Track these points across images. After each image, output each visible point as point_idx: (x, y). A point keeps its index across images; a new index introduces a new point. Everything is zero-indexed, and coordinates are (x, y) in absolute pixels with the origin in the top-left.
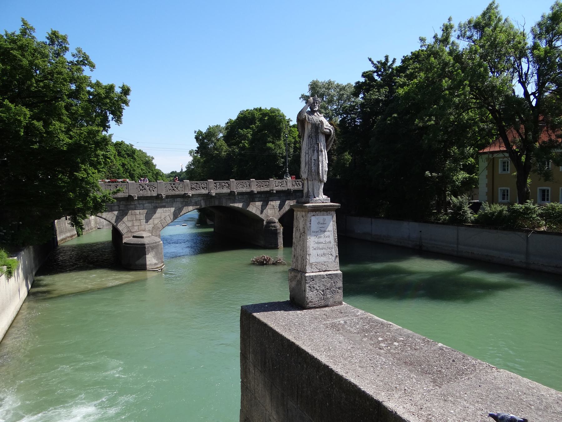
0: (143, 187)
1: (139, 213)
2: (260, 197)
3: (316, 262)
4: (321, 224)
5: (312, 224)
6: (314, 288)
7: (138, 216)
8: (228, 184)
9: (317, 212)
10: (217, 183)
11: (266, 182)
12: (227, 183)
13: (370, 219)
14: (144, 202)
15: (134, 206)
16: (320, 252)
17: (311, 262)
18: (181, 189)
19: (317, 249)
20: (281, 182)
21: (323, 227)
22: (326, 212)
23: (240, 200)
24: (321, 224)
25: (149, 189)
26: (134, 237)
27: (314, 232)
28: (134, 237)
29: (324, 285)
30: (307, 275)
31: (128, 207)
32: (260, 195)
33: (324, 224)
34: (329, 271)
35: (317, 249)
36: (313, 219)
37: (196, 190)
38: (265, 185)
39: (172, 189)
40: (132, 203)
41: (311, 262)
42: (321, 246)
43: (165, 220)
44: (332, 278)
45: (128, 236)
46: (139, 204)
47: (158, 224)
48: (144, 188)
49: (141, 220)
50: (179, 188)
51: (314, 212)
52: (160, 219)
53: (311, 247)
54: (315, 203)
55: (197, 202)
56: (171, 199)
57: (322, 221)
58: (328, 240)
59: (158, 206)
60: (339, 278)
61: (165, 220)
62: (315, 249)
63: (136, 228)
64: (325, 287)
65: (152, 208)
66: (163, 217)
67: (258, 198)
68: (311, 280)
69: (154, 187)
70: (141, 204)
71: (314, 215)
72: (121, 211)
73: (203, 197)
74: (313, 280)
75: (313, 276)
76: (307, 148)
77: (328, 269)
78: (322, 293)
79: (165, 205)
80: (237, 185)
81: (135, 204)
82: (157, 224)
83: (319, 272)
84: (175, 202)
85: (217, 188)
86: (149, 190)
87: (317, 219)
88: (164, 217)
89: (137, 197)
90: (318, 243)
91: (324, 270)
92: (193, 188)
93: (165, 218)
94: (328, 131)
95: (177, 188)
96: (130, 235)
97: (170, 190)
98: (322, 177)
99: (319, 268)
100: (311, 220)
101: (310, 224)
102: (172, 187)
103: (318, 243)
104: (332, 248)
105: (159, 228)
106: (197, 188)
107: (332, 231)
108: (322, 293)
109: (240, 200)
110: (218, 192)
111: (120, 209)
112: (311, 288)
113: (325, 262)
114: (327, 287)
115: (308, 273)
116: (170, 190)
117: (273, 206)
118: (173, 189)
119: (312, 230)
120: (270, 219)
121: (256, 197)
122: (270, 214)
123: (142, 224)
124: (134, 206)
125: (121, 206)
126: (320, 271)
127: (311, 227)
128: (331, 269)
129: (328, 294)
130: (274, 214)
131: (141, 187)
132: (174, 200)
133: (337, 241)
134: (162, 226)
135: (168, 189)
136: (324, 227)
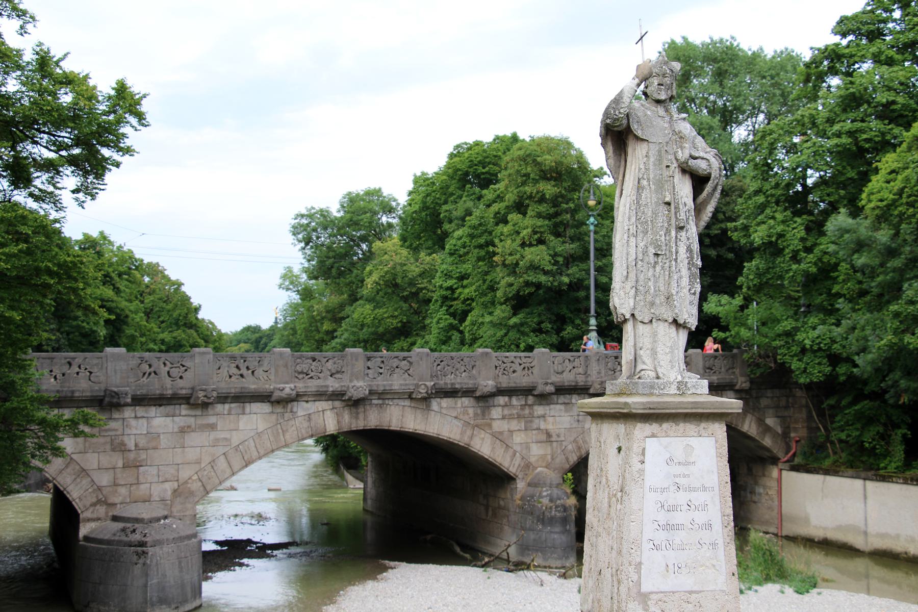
0: (150, 366)
1: (136, 445)
2: (506, 405)
3: (662, 592)
5: (647, 465)
7: (132, 456)
8: (408, 361)
10: (375, 357)
11: (525, 357)
12: (404, 359)
13: (859, 483)
14: (153, 411)
15: (120, 422)
17: (645, 588)
18: (265, 375)
19: (664, 548)
20: (572, 359)
21: (684, 476)
23: (444, 411)
25: (168, 372)
26: (115, 519)
28: (115, 519)
32: (507, 398)
33: (687, 464)
35: (664, 548)
36: (652, 445)
37: (311, 378)
38: (522, 366)
39: (239, 373)
40: (116, 415)
42: (679, 537)
43: (212, 467)
45: (95, 516)
46: (136, 417)
47: (190, 481)
48: (152, 369)
49: (141, 468)
50: (259, 372)
52: (197, 467)
53: (645, 539)
55: (312, 416)
56: (233, 405)
57: (679, 455)
58: (700, 517)
59: (193, 426)
61: (212, 467)
62: (657, 547)
63: (123, 491)
65: (176, 430)
66: (206, 460)
67: (500, 409)
69: (183, 366)
71: (653, 436)
73: (330, 402)
76: (633, 219)
79: (213, 424)
80: (435, 364)
81: (123, 419)
82: (186, 482)
84: (244, 414)
85: (376, 375)
86: (169, 376)
87: (666, 447)
88: (210, 459)
89: (130, 396)
90: (669, 527)
92: (302, 373)
93: (212, 463)
95: (253, 372)
96: (101, 510)
97: (230, 377)
100: (644, 449)
102: (238, 367)
103: (669, 527)
104: (714, 545)
105: (192, 493)
106: (312, 374)
107: (716, 489)
109: (444, 411)
110: (378, 386)
113: (691, 592)
116: (230, 377)
117: (549, 435)
118: (242, 376)
119: (647, 484)
120: (538, 474)
121: (494, 406)
122: (538, 461)
123: (142, 479)
124: (120, 422)
127: (647, 472)
130: (550, 460)
131: (145, 367)
132: (244, 408)
134: (202, 489)
135: (226, 373)
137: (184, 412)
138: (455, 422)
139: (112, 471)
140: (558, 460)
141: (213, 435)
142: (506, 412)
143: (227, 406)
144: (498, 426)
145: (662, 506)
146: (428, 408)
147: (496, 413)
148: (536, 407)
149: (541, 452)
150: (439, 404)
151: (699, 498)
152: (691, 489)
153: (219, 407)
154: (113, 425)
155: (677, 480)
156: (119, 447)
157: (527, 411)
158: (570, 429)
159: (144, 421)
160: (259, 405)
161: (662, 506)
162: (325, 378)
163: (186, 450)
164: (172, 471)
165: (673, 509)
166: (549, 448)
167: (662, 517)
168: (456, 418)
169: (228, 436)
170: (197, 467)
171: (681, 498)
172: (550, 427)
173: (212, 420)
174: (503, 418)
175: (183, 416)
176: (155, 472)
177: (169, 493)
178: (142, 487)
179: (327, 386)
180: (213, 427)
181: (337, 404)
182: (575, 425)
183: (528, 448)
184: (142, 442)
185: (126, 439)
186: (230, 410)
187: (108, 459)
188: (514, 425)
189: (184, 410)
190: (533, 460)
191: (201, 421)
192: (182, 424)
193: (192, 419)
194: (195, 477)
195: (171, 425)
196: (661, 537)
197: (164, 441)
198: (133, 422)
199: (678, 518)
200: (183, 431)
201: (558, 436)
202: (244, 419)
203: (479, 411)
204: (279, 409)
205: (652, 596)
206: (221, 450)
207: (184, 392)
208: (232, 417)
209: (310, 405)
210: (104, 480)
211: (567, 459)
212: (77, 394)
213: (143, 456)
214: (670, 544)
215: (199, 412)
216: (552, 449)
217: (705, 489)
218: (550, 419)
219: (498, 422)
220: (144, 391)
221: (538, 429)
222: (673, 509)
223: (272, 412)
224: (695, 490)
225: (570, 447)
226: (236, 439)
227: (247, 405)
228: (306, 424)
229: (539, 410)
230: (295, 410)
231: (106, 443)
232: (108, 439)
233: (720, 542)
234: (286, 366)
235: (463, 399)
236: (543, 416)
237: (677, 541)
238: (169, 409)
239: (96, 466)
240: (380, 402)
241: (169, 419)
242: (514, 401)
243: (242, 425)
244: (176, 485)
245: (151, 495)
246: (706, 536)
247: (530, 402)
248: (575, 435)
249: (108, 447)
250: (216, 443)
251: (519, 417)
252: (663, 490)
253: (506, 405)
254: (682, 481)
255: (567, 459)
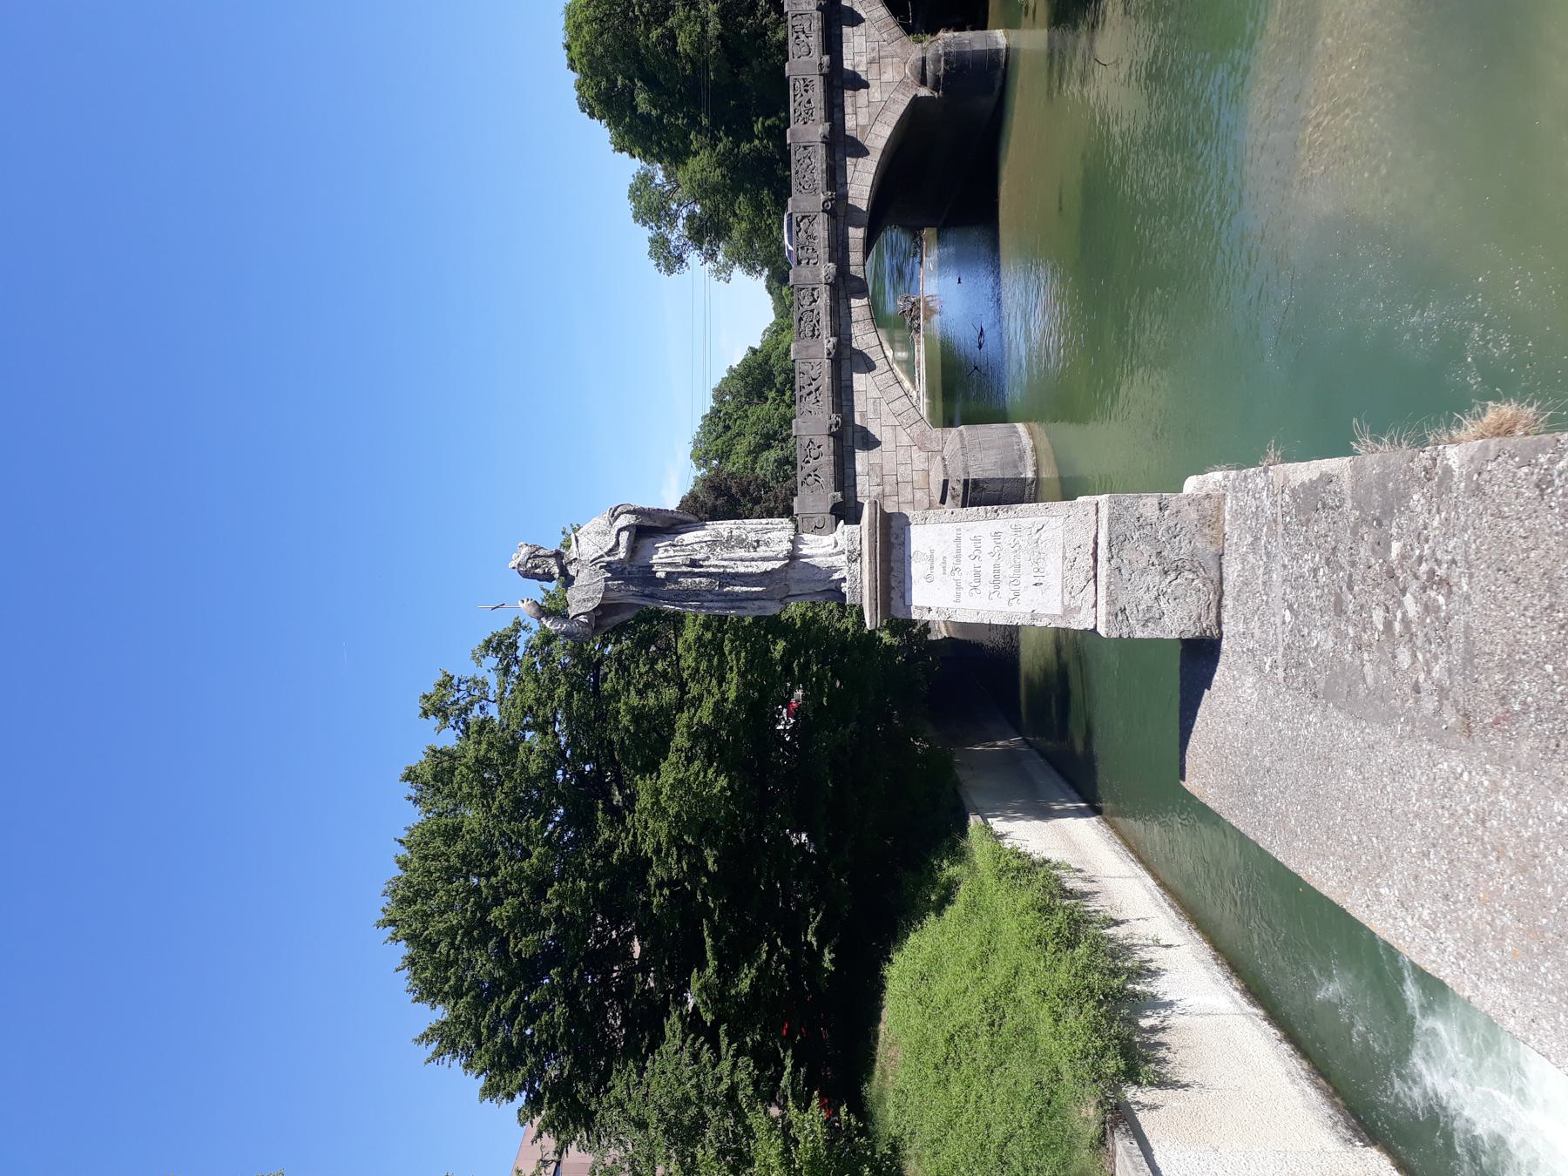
4: (932, 568)
6: (1149, 608)
9: (893, 584)
16: (1027, 579)
19: (1017, 588)
21: (944, 563)
22: (894, 552)
24: (932, 568)
27: (958, 595)
29: (1144, 571)
30: (1102, 631)
33: (932, 558)
34: (1096, 544)
35: (1017, 588)
41: (1059, 611)
42: (1007, 571)
44: (1121, 538)
51: (893, 595)
53: (1008, 609)
54: (861, 582)
58: (988, 544)
60: (1127, 508)
64: (1153, 564)
68: (1120, 618)
74: (1123, 610)
75: (1109, 613)
77: (1092, 545)
78: (1173, 575)
83: (1096, 582)
90: (996, 582)
91: (1091, 562)
94: (625, 536)
98: (776, 559)
99: (1082, 578)
101: (930, 610)
103: (996, 582)
104: (1017, 529)
108: (1173, 575)
112: (1147, 621)
113: (1065, 558)
114: (1153, 558)
115: (1096, 625)
119: (952, 605)
126: (1095, 576)
128: (1094, 533)
129: (1178, 554)
133: (996, 507)
136: (945, 557)
145: (975, 588)
151: (967, 547)
152: (958, 557)
155: (948, 570)
161: (975, 588)
165: (977, 575)
167: (985, 588)
171: (967, 566)
196: (1006, 590)
199: (987, 570)
205: (1066, 603)
214: (1015, 581)
217: (958, 539)
222: (977, 575)
224: (959, 551)
233: (1013, 522)
237: (1011, 572)
246: (1007, 538)
252: (959, 587)
254: (950, 565)
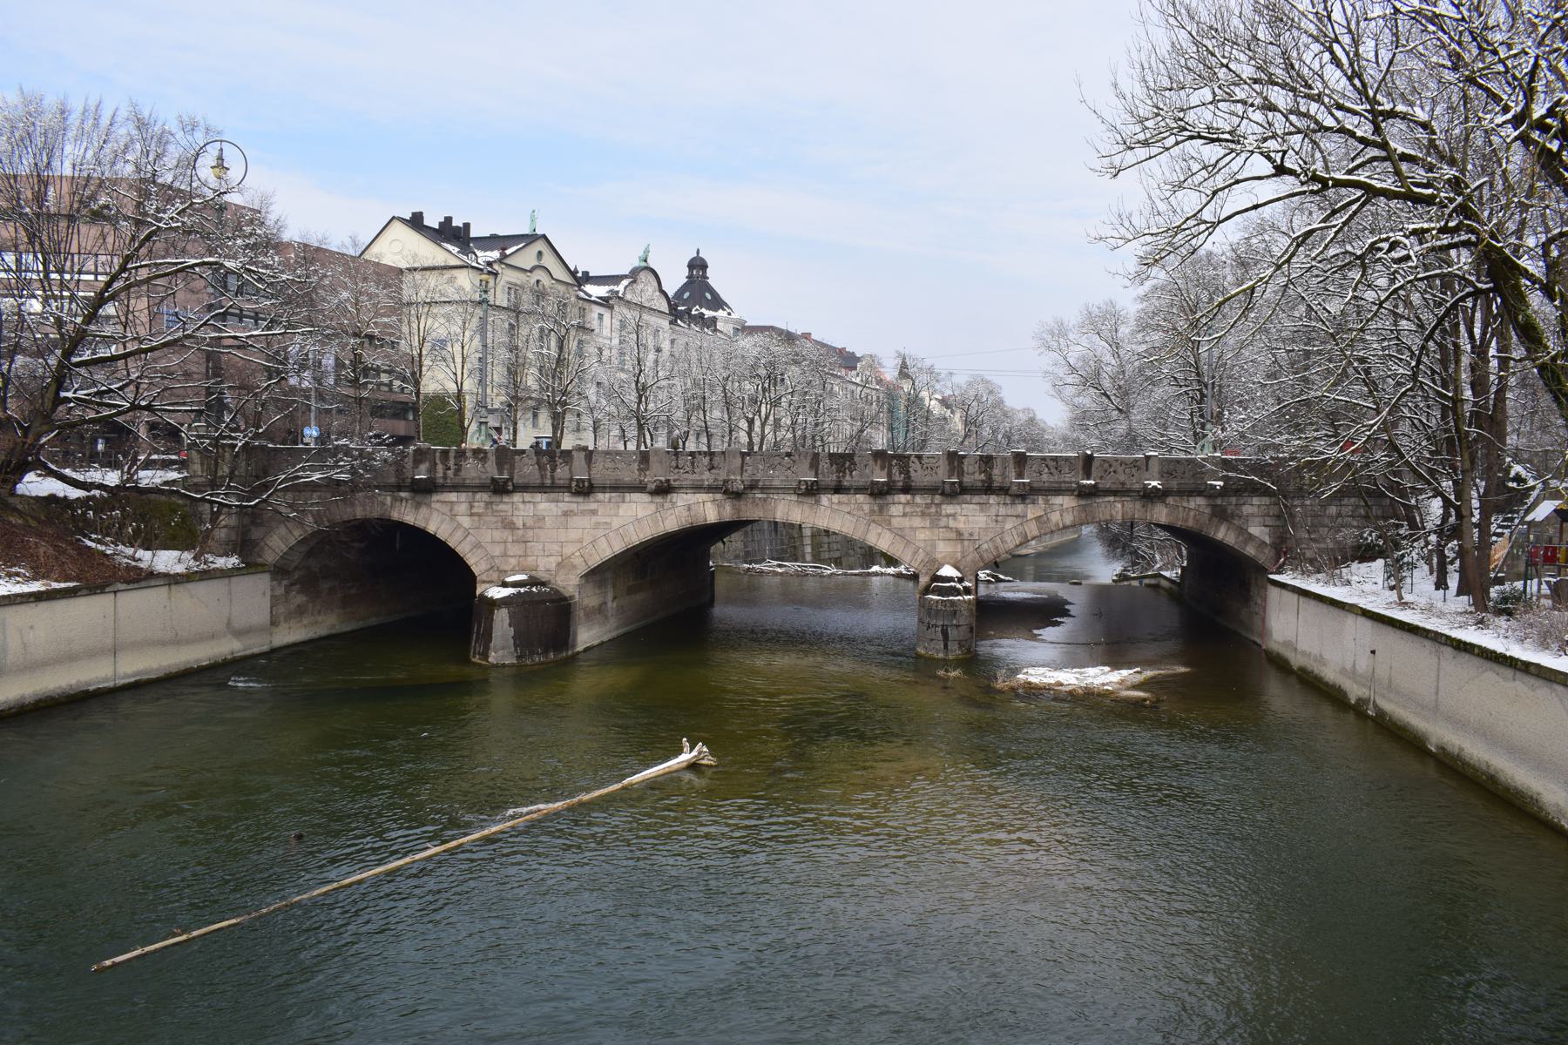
1: (524, 525)
2: (908, 503)
7: (520, 532)
14: (538, 497)
15: (510, 505)
31: (494, 507)
40: (506, 499)
46: (524, 502)
52: (579, 546)
56: (613, 494)
65: (560, 514)
66: (588, 539)
67: (901, 507)
70: (529, 502)
72: (476, 518)
82: (569, 557)
84: (623, 502)
111: (475, 510)
123: (529, 553)
124: (510, 505)
125: (476, 504)
132: (624, 497)
137: (567, 499)
138: (848, 516)
139: (502, 545)
140: (969, 558)
141: (594, 519)
142: (908, 509)
143: (607, 495)
144: (896, 522)
146: (818, 502)
147: (896, 510)
148: (944, 506)
149: (950, 549)
150: (830, 500)
153: (600, 496)
154: (502, 507)
156: (510, 526)
157: (933, 510)
158: (986, 529)
159: (532, 506)
160: (639, 495)
162: (701, 473)
163: (569, 530)
164: (556, 547)
166: (959, 546)
168: (849, 513)
169: (608, 520)
170: (579, 546)
172: (961, 526)
173: (593, 506)
174: (905, 515)
175: (567, 502)
176: (541, 547)
177: (554, 565)
178: (530, 559)
179: (703, 480)
180: (594, 512)
181: (719, 496)
182: (993, 525)
183: (934, 546)
184: (530, 523)
185: (515, 519)
186: (610, 499)
187: (498, 535)
188: (917, 522)
189: (567, 497)
190: (938, 556)
191: (583, 507)
192: (565, 509)
193: (575, 505)
194: (578, 554)
195: (555, 509)
197: (548, 522)
198: (521, 506)
200: (566, 514)
201: (971, 535)
202: (624, 507)
203: (876, 508)
204: (658, 499)
206: (601, 532)
207: (562, 482)
208: (612, 505)
209: (689, 496)
210: (497, 550)
211: (981, 557)
212: (467, 481)
213: (530, 533)
215: (580, 499)
216: (963, 547)
218: (962, 519)
219: (899, 519)
220: (526, 481)
221: (947, 527)
223: (652, 502)
225: (985, 546)
226: (616, 523)
227: (627, 495)
228: (685, 514)
229: (948, 509)
230: (674, 500)
231: (497, 522)
232: (500, 519)
234: (661, 462)
235: (858, 496)
236: (953, 515)
238: (553, 495)
239: (489, 540)
240: (765, 496)
241: (553, 505)
242: (918, 499)
243: (621, 512)
244: (560, 559)
245: (537, 566)
247: (936, 501)
248: (992, 535)
249: (500, 524)
250: (597, 526)
251: (923, 514)
253: (908, 503)
255: (981, 557)
